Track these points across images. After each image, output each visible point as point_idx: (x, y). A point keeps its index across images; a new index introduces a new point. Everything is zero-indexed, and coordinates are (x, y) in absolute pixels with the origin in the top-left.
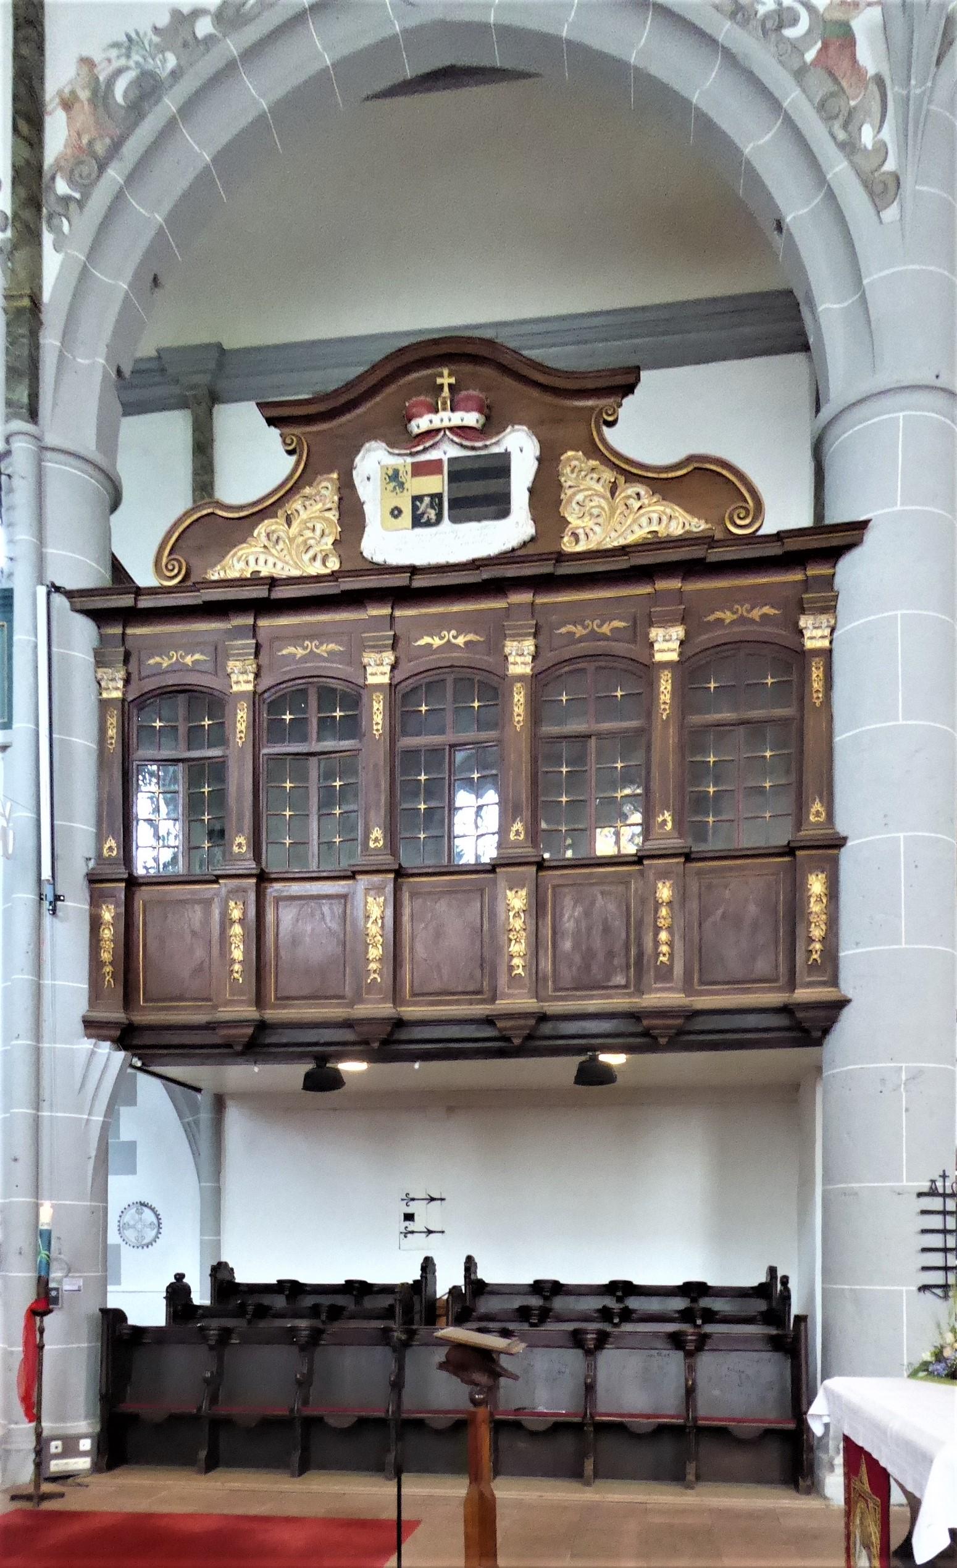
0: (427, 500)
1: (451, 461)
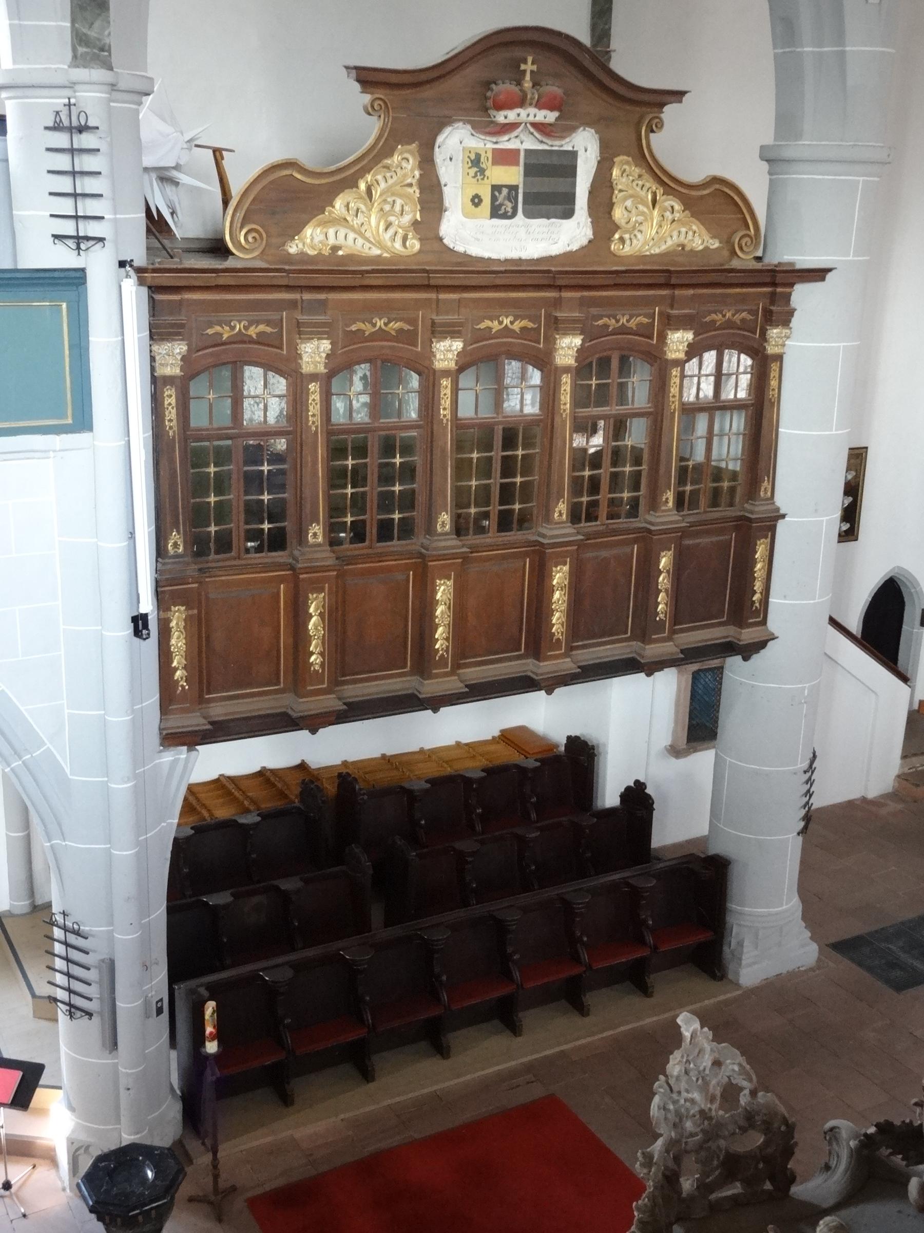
0: (505, 191)
1: (527, 152)
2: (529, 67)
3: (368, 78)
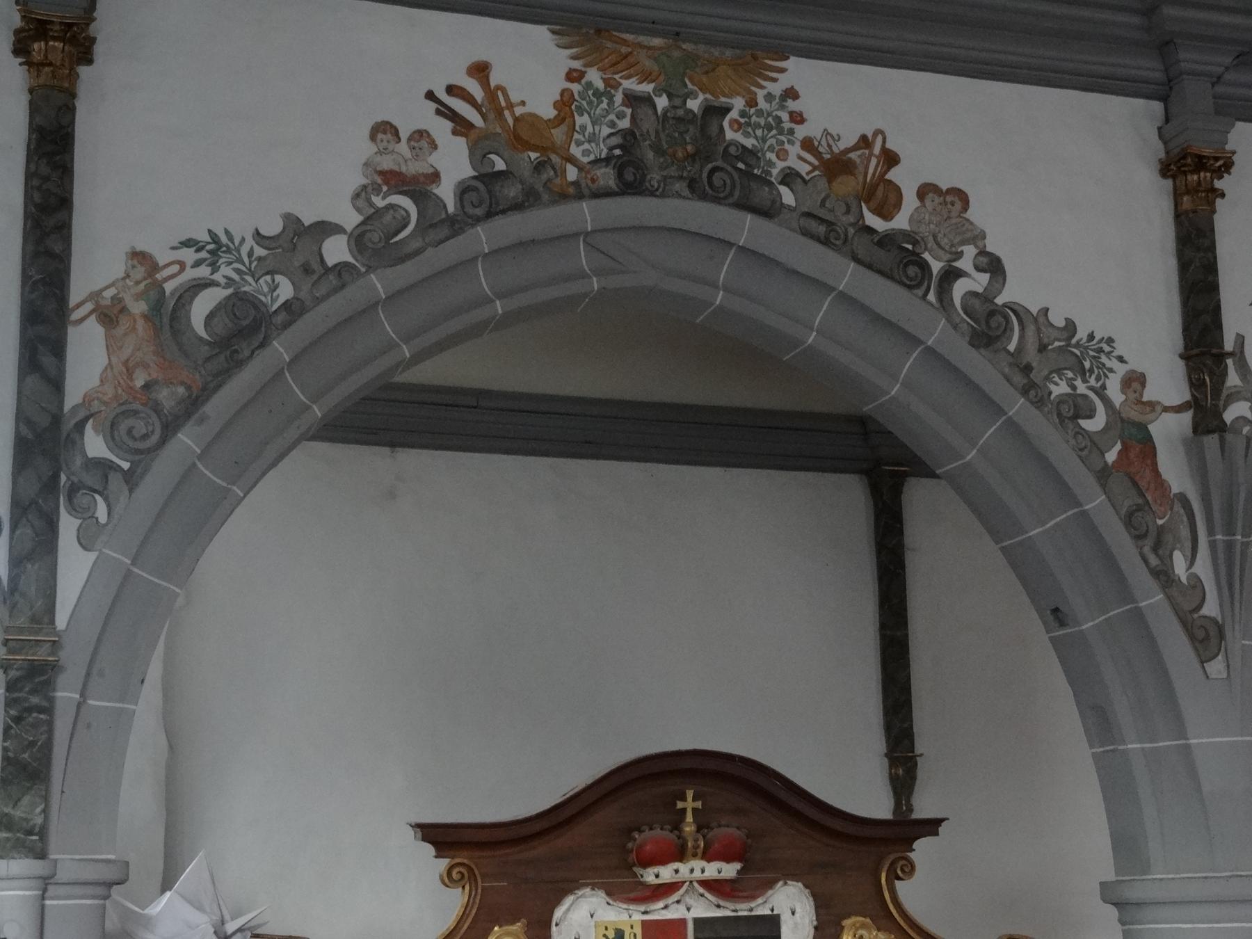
2: (689, 804)
3: (441, 837)
